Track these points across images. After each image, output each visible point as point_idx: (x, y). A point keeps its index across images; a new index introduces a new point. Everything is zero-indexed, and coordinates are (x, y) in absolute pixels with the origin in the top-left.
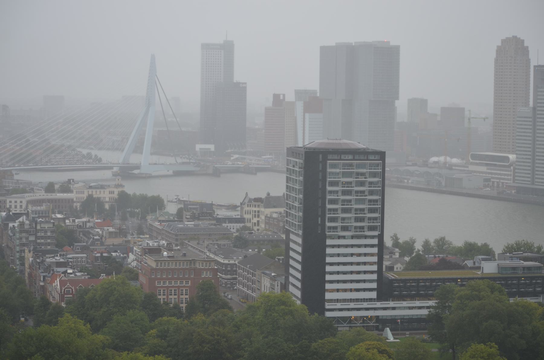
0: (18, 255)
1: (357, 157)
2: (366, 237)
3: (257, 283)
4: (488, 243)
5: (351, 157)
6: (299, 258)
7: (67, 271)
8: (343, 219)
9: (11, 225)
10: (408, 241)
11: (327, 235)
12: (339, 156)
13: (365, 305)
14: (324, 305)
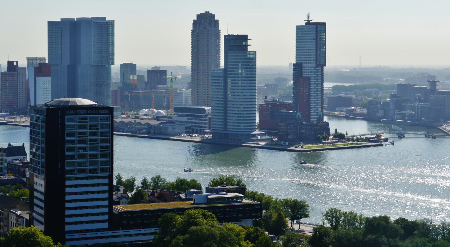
1: (89, 112)
2: (98, 178)
4: (196, 179)
7: (177, 196)
8: (79, 163)
10: (130, 180)
11: (66, 177)
13: (99, 234)
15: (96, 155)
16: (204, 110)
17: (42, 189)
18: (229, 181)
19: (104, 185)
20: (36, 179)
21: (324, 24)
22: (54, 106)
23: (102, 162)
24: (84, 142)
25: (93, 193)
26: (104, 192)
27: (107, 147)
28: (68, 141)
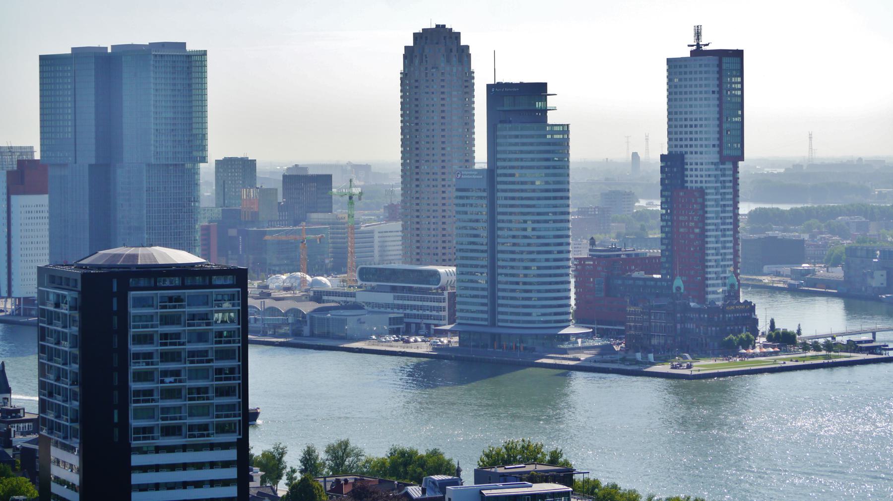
1: (188, 282)
2: (212, 447)
4: (441, 450)
5: (177, 281)
8: (165, 410)
10: (271, 453)
11: (132, 446)
12: (207, 278)
15: (205, 390)
16: (436, 274)
18: (531, 454)
19: (226, 464)
20: (56, 453)
21: (738, 54)
22: (99, 267)
23: (219, 407)
24: (174, 357)
26: (226, 483)
27: (232, 370)
28: (137, 356)
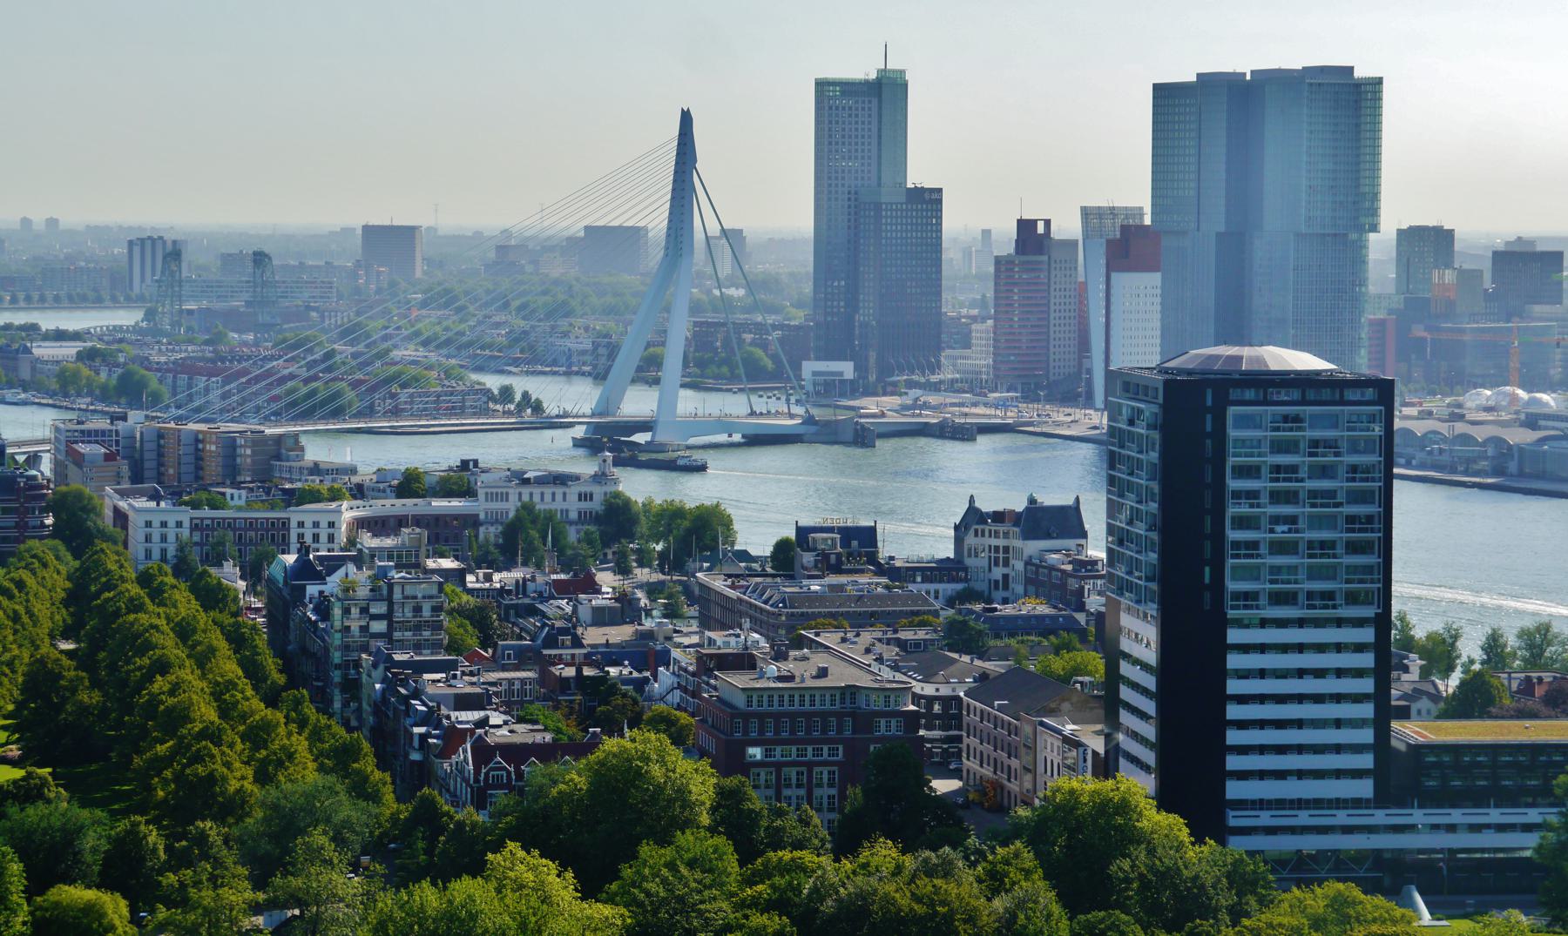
0: (337, 676)
1: (1311, 395)
2: (1339, 622)
3: (1023, 750)
5: (1296, 394)
6: (1150, 682)
8: (1275, 570)
9: (312, 590)
13: (1342, 817)
14: (1223, 817)
17: (1151, 656)
19: (1359, 648)
20: (1126, 620)
22: (1189, 372)
23: (1352, 569)
24: (1290, 497)
25: (1320, 673)
26: (1359, 673)
27: (1370, 519)
28: (1237, 495)
